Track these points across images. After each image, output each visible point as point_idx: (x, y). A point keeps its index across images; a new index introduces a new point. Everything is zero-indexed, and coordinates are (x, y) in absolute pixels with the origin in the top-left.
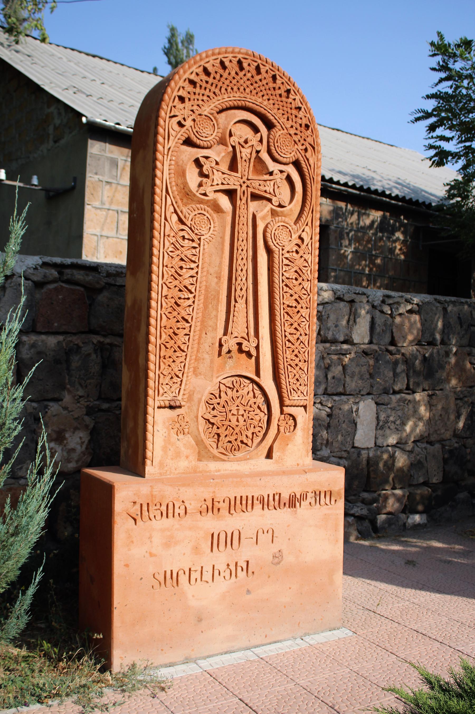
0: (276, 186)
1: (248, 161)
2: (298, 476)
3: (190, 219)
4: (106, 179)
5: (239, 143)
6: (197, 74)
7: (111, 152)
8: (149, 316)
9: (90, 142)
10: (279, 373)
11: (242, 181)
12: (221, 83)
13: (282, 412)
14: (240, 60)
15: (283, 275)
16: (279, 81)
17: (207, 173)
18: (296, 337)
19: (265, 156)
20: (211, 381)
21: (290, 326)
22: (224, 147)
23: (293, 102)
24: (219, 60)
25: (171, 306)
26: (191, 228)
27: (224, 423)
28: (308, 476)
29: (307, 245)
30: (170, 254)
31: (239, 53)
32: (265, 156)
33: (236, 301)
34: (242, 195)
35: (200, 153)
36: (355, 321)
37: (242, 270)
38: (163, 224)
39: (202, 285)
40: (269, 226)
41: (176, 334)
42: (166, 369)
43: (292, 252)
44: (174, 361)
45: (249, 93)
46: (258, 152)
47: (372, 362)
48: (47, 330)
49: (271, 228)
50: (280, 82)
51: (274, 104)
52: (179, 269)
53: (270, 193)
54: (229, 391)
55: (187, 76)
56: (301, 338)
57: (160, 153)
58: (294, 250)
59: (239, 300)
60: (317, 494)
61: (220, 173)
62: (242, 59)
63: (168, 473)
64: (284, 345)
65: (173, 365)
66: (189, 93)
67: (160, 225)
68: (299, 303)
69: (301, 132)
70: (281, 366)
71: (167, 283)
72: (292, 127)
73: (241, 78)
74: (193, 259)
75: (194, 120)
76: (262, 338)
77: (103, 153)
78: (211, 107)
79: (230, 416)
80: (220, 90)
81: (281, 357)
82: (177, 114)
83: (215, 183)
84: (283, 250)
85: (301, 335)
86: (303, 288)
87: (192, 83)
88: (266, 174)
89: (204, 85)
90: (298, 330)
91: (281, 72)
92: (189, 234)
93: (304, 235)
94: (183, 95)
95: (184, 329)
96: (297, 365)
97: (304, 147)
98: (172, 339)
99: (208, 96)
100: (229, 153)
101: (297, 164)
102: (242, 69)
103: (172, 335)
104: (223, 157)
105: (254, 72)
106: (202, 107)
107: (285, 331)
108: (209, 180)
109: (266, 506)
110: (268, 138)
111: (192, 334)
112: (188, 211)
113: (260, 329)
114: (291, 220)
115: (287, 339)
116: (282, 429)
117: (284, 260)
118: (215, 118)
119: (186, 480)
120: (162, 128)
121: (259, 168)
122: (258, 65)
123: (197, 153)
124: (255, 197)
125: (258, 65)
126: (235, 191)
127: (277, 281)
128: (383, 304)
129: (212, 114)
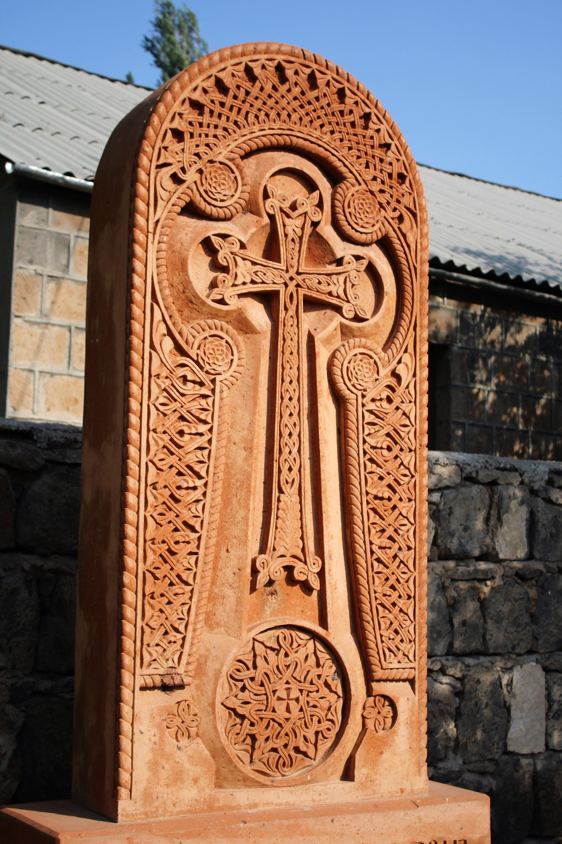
0: (349, 285)
1: (297, 241)
2: (402, 813)
3: (196, 346)
4: (49, 270)
5: (282, 210)
6: (205, 91)
7: (58, 223)
8: (123, 520)
9: (19, 206)
10: (362, 619)
11: (287, 276)
12: (247, 105)
13: (369, 692)
14: (279, 63)
15: (365, 442)
16: (349, 100)
17: (225, 264)
18: (391, 553)
19: (327, 231)
20: (239, 637)
21: (379, 534)
22: (255, 218)
23: (375, 135)
24: (244, 64)
25: (164, 503)
26: (197, 362)
27: (263, 714)
28: (422, 812)
29: (407, 387)
30: (162, 408)
31: (279, 52)
32: (327, 231)
33: (281, 491)
34: (288, 301)
36: (499, 519)
37: (290, 435)
38: (147, 356)
39: (219, 463)
40: (338, 355)
41: (173, 553)
42: (155, 618)
43: (381, 400)
44: (169, 603)
45: (298, 122)
46: (315, 224)
47: (533, 593)
49: (341, 359)
50: (352, 101)
51: (341, 140)
52: (178, 436)
53: (338, 297)
54: (271, 656)
55: (186, 94)
56: (401, 555)
57: (141, 230)
58: (384, 396)
61: (248, 263)
62: (283, 63)
63: (160, 811)
64: (370, 569)
65: (168, 609)
66: (191, 124)
67: (143, 358)
68: (395, 492)
69: (391, 187)
70: (366, 607)
71: (156, 460)
72: (375, 179)
73: (283, 97)
74: (203, 417)
75: (200, 171)
77: (43, 226)
78: (230, 148)
79: (274, 702)
80: (246, 119)
81: (364, 591)
82: (170, 161)
83: (239, 281)
84: (363, 396)
85: (400, 549)
86: (402, 463)
87: (197, 106)
88: (330, 263)
89: (217, 109)
90: (394, 541)
91: (352, 84)
92: (194, 372)
93: (401, 370)
94: (180, 128)
95: (188, 543)
96: (394, 604)
97: (397, 214)
98: (166, 562)
99: (225, 129)
100: (263, 227)
101: (385, 244)
102: (283, 79)
103: (166, 555)
104: (253, 234)
105: (305, 85)
106: (215, 149)
107: (371, 543)
110: (333, 199)
111: (201, 552)
112: (191, 332)
113: (326, 539)
114: (378, 343)
115: (375, 556)
116: (370, 724)
118: (238, 167)
120: (144, 185)
121: (318, 252)
122: (313, 72)
123: (208, 230)
124: (311, 304)
125: (313, 72)
126: (278, 292)
127: (354, 453)
128: (550, 487)
129: (232, 160)
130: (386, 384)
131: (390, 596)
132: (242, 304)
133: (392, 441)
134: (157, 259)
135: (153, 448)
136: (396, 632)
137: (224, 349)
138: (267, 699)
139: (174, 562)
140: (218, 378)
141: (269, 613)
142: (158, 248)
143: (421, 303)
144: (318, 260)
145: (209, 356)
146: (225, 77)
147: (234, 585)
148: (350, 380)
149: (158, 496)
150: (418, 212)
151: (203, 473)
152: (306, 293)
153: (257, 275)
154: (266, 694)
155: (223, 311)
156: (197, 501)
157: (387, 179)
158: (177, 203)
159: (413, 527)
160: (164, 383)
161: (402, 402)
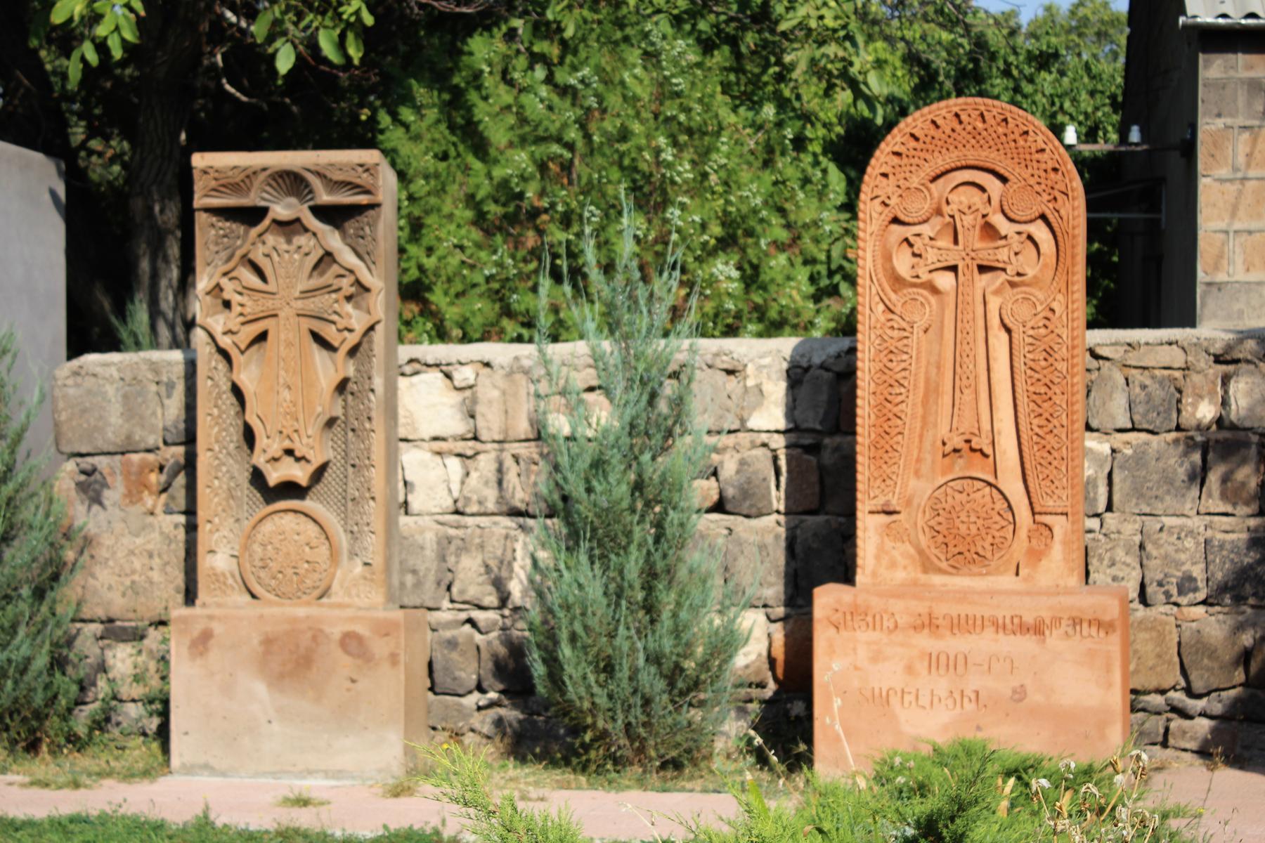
4: (1241, 121)
11: (964, 254)
28: (1062, 599)
35: (908, 232)
54: (957, 496)
55: (889, 149)
56: (1055, 431)
58: (1041, 324)
59: (966, 391)
60: (1076, 622)
70: (1027, 466)
76: (999, 433)
77: (1232, 73)
79: (957, 522)
87: (898, 154)
93: (1055, 305)
109: (1001, 630)
119: (899, 593)
124: (983, 269)
146: (916, 132)
150: (1070, 194)
151: (906, 384)
157: (1043, 174)
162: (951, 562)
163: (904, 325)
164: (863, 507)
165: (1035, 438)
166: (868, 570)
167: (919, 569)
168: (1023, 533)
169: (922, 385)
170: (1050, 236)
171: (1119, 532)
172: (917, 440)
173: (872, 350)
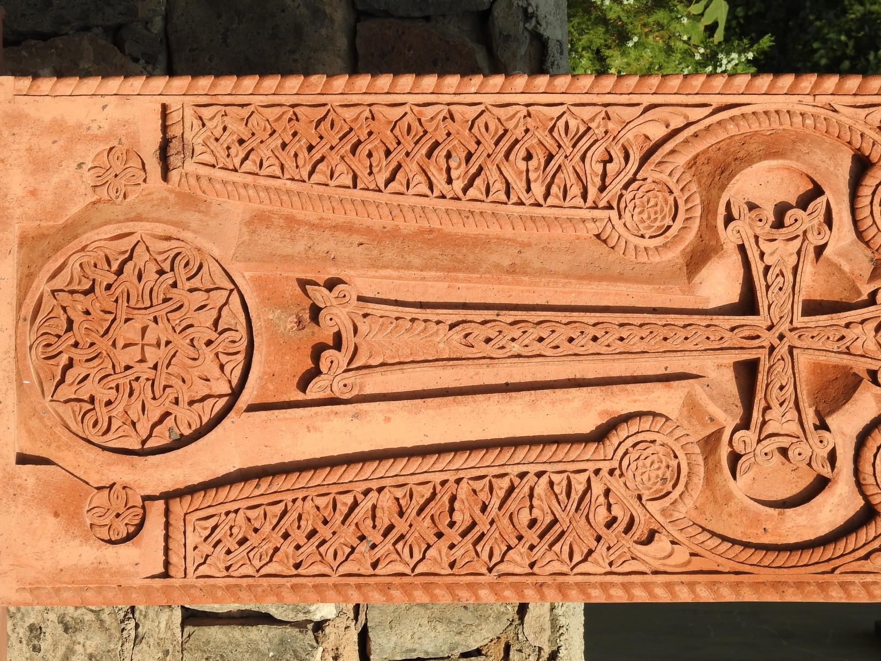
3: (657, 176)
11: (784, 327)
15: (539, 475)
17: (787, 221)
20: (235, 258)
26: (633, 180)
30: (561, 124)
33: (452, 326)
34: (746, 333)
48: (361, 51)
52: (523, 153)
53: (764, 423)
54: (207, 317)
56: (364, 547)
58: (616, 511)
59: (457, 335)
68: (464, 535)
70: (280, 483)
74: (554, 189)
76: (356, 416)
79: (142, 319)
88: (818, 413)
90: (385, 535)
92: (619, 174)
93: (661, 544)
95: (371, 173)
96: (286, 536)
98: (341, 139)
104: (840, 270)
107: (380, 490)
108: (768, 226)
111: (357, 194)
117: (583, 477)
121: (832, 392)
123: (835, 192)
124: (747, 373)
130: (635, 514)
131: (299, 527)
132: (729, 251)
133: (543, 527)
134: (777, 112)
135: (502, 113)
136: (242, 542)
137: (658, 224)
138: (146, 308)
139: (343, 151)
140: (614, 214)
141: (271, 317)
142: (794, 112)
143: (776, 585)
144: (820, 395)
145: (645, 199)
147: (310, 252)
148: (634, 446)
149: (435, 122)
151: (472, 193)
152: (762, 363)
153: (777, 275)
154: (152, 306)
155: (716, 220)
156: (431, 187)
158: (865, 140)
159: (408, 571)
160: (598, 127)
161: (609, 548)
162: (49, 303)
163: (615, 188)
164: (177, 91)
165: (349, 499)
166: (27, 105)
167: (30, 225)
168: (120, 471)
169: (471, 229)
170: (823, 531)
171: (138, 640)
172: (339, 218)
173: (556, 111)
